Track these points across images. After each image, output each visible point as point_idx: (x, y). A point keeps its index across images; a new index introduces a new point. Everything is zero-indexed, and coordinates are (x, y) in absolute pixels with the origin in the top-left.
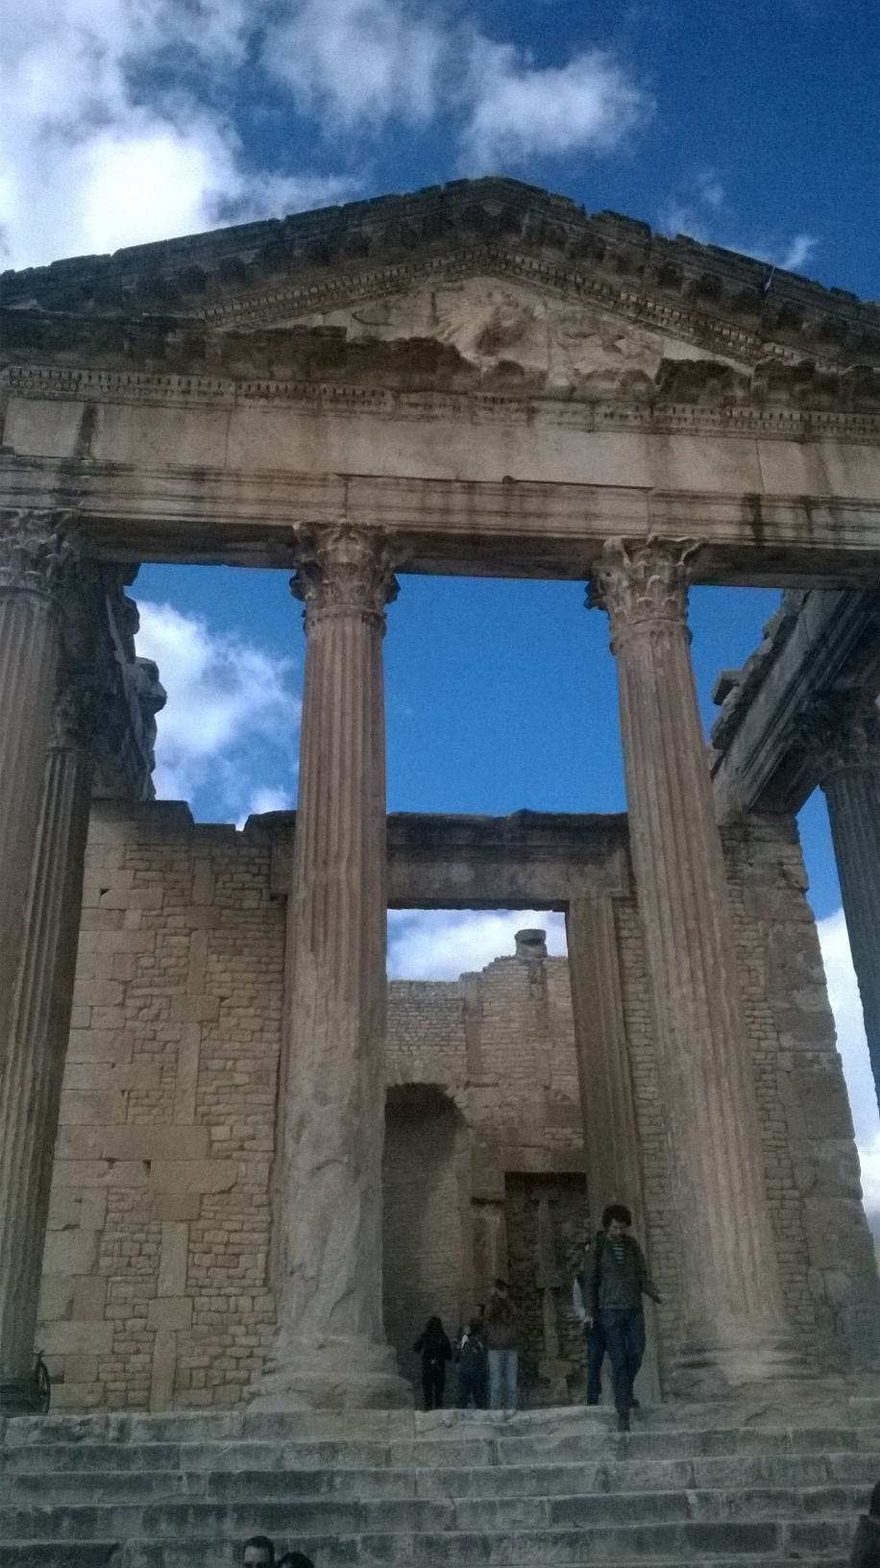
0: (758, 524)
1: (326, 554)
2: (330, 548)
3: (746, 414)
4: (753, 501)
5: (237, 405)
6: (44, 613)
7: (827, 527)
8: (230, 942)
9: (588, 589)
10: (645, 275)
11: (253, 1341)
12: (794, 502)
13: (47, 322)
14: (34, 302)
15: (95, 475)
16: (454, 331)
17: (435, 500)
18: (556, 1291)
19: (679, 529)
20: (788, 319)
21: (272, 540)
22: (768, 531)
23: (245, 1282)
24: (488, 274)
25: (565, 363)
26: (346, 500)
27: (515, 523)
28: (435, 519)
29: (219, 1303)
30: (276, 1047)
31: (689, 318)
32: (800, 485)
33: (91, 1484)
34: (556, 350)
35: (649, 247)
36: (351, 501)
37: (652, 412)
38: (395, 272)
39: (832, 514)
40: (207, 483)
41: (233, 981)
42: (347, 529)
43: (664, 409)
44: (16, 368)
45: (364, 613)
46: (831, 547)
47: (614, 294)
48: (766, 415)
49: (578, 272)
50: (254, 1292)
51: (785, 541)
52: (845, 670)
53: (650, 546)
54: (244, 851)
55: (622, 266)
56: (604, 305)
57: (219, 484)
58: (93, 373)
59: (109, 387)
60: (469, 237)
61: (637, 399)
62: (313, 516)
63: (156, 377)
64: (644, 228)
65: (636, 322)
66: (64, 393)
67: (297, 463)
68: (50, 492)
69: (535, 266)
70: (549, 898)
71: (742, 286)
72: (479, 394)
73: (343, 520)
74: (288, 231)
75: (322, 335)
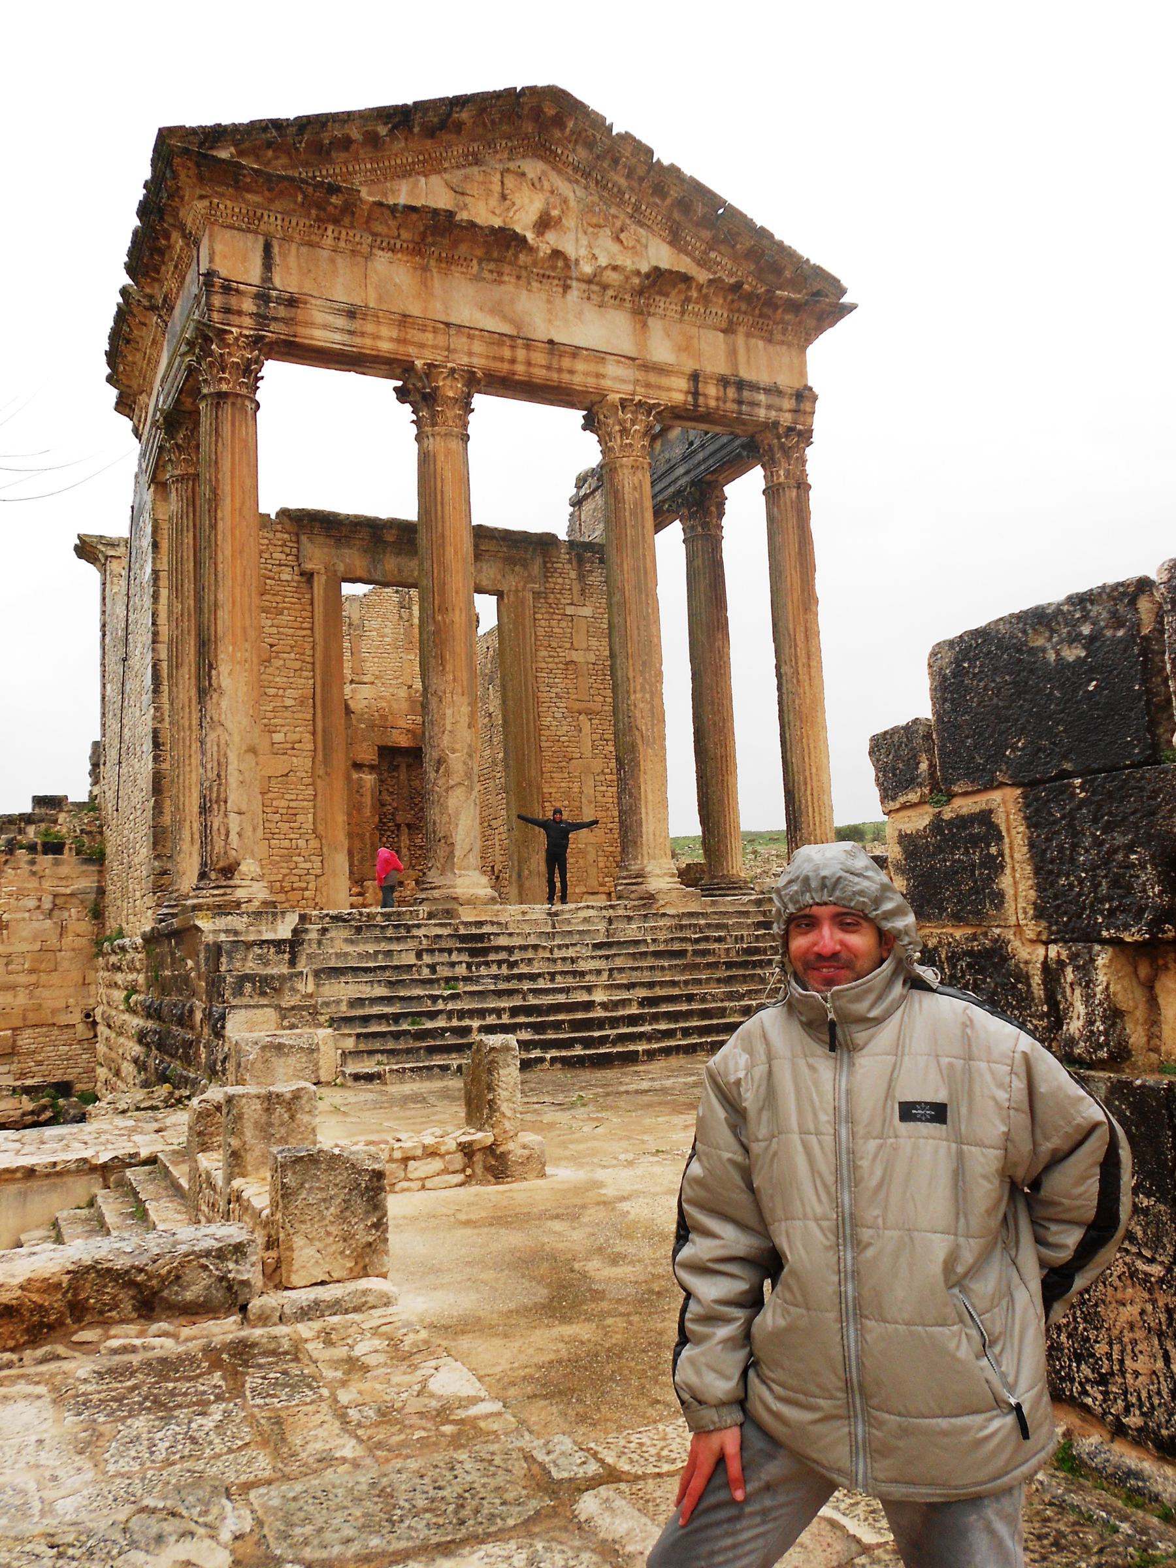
0: (696, 394)
1: (437, 388)
2: (441, 384)
4: (695, 377)
5: (371, 254)
7: (734, 401)
8: (274, 604)
11: (308, 865)
14: (232, 149)
15: (279, 304)
17: (507, 353)
18: (409, 826)
22: (701, 400)
23: (302, 831)
27: (555, 376)
28: (506, 366)
29: (286, 843)
30: (311, 682)
33: (377, 940)
36: (452, 347)
41: (278, 633)
42: (453, 370)
43: (648, 298)
44: (216, 201)
47: (621, 192)
50: (307, 837)
54: (279, 535)
60: (529, 127)
61: (632, 288)
62: (429, 356)
64: (649, 152)
65: (632, 217)
66: (250, 225)
67: (415, 310)
70: (490, 588)
73: (449, 365)
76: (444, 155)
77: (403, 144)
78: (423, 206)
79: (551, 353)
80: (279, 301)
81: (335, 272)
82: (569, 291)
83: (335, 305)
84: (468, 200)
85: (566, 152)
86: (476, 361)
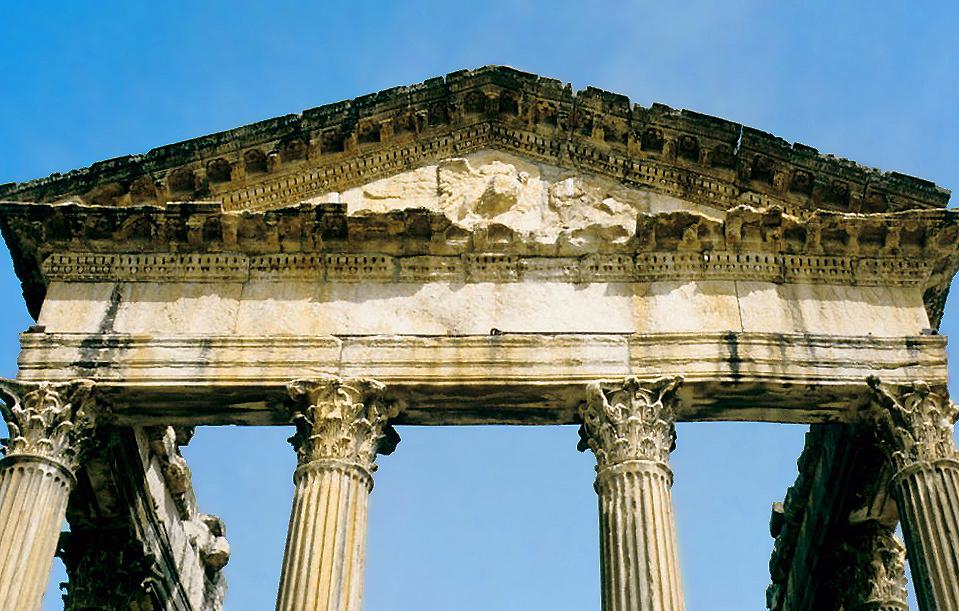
0: (734, 361)
3: (723, 258)
4: (731, 338)
9: (581, 432)
10: (630, 141)
19: (658, 370)
20: (762, 174)
22: (744, 368)
27: (500, 372)
28: (424, 372)
31: (672, 176)
32: (781, 325)
34: (548, 212)
35: (630, 116)
37: (635, 263)
42: (336, 385)
44: (57, 256)
45: (348, 466)
48: (743, 258)
49: (571, 141)
51: (760, 377)
53: (626, 389)
55: (609, 136)
56: (594, 168)
57: (223, 349)
58: (123, 256)
62: (308, 375)
63: (179, 256)
64: (623, 100)
65: (624, 181)
68: (71, 365)
69: (532, 140)
71: (716, 143)
72: (472, 255)
74: (305, 124)
75: (324, 211)
76: (361, 165)
80: (113, 343)
82: (526, 273)
85: (525, 134)
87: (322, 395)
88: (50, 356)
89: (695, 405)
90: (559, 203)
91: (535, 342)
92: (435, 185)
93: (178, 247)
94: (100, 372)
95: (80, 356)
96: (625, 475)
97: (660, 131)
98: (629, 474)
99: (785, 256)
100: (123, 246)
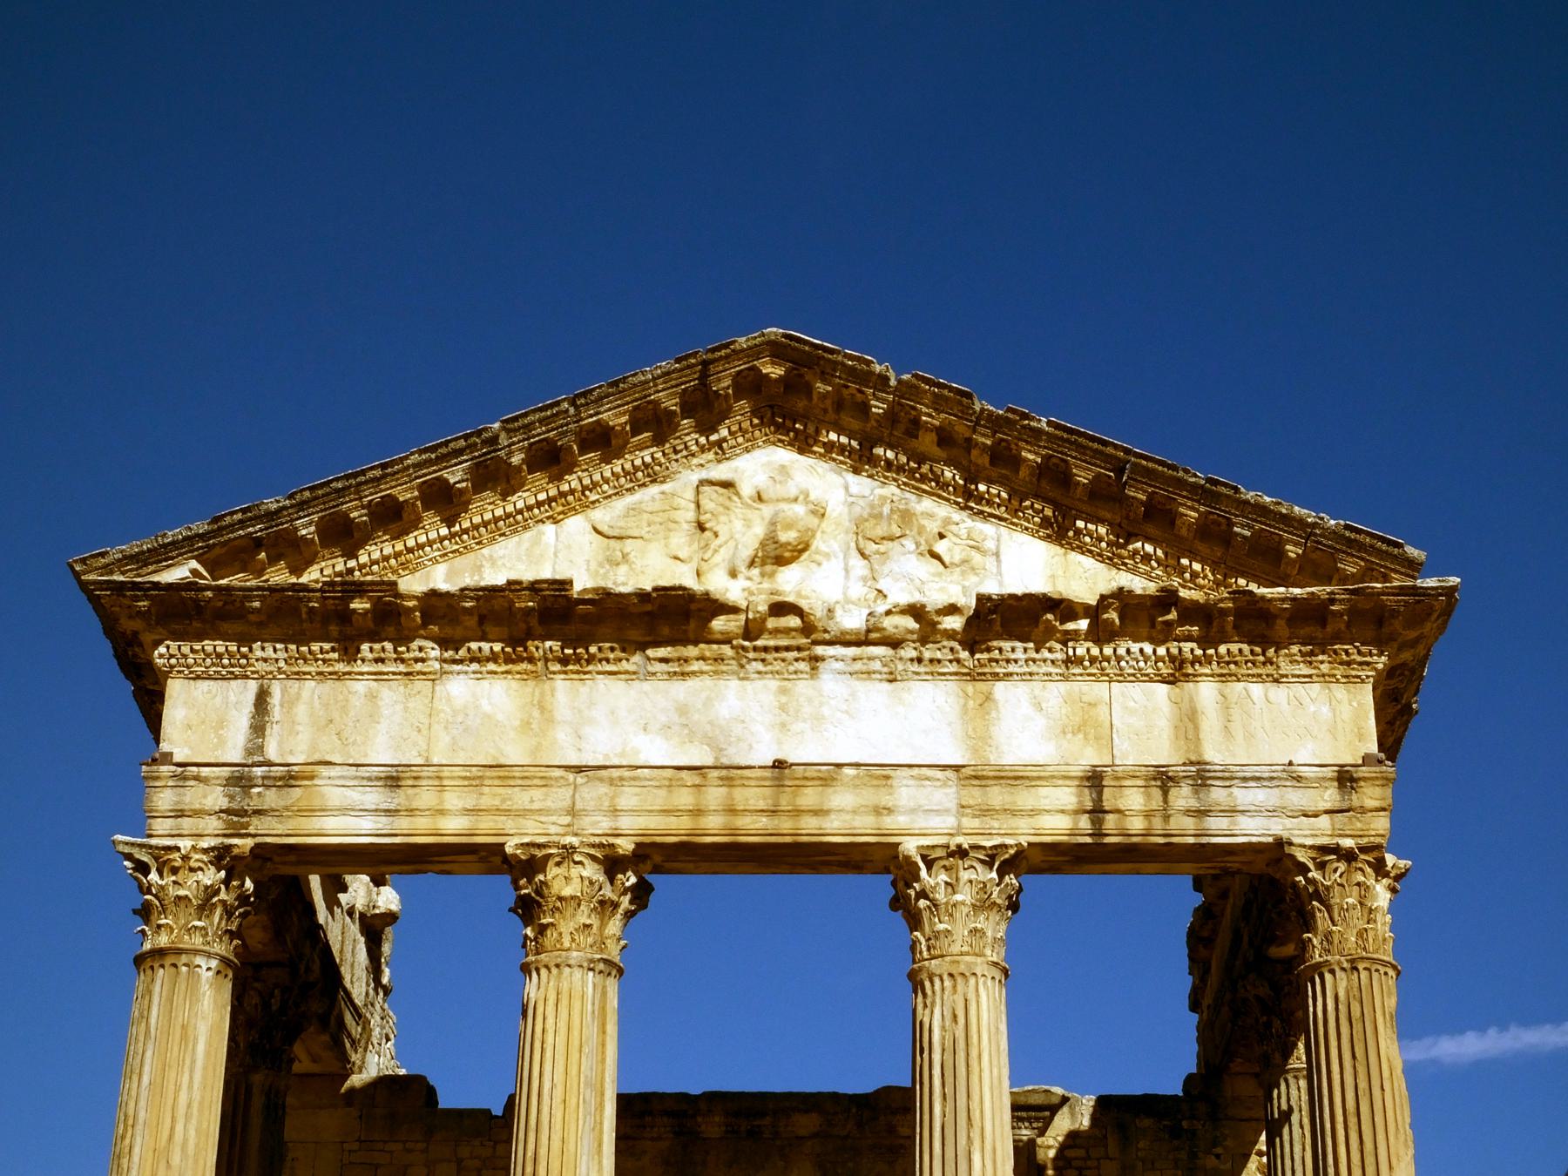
0: (1097, 812)
4: (1094, 780)
6: (210, 973)
7: (1188, 812)
9: (894, 884)
12: (1147, 779)
13: (209, 594)
14: (194, 564)
15: (268, 787)
16: (720, 546)
19: (996, 825)
21: (484, 854)
22: (1110, 822)
24: (774, 444)
25: (864, 579)
26: (574, 803)
27: (785, 825)
32: (1164, 752)
36: (579, 806)
38: (648, 459)
39: (1196, 792)
40: (400, 792)
42: (569, 851)
45: (592, 961)
46: (1191, 840)
52: (1275, 941)
56: (924, 487)
58: (266, 645)
59: (285, 660)
65: (962, 509)
67: (514, 753)
68: (216, 813)
73: (568, 840)
77: (504, 485)
78: (510, 583)
79: (779, 784)
81: (374, 717)
83: (363, 772)
84: (629, 545)
86: (627, 823)
87: (551, 863)
88: (187, 799)
89: (1043, 861)
90: (870, 548)
91: (833, 779)
92: (691, 515)
93: (341, 632)
94: (256, 825)
95: (226, 799)
96: (945, 977)
97: (1017, 445)
98: (951, 975)
99: (1182, 644)
100: (264, 632)
